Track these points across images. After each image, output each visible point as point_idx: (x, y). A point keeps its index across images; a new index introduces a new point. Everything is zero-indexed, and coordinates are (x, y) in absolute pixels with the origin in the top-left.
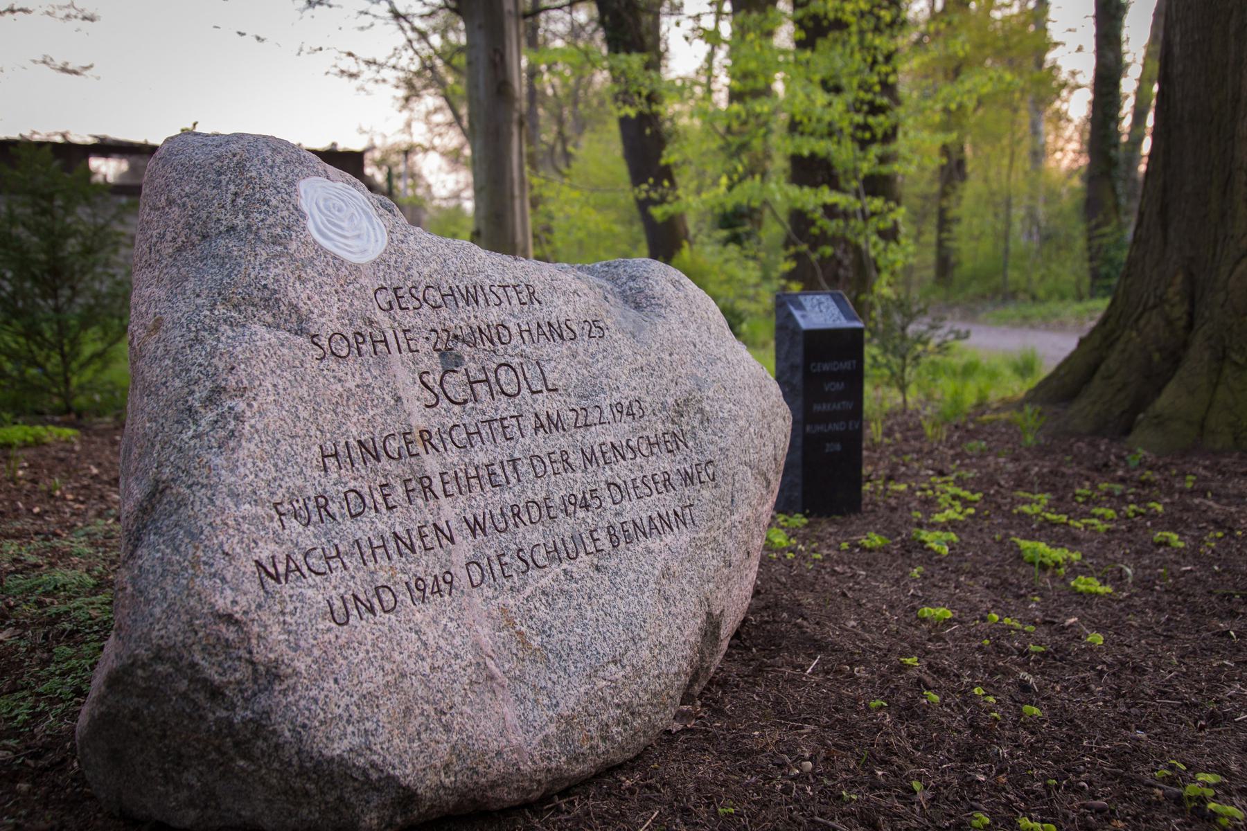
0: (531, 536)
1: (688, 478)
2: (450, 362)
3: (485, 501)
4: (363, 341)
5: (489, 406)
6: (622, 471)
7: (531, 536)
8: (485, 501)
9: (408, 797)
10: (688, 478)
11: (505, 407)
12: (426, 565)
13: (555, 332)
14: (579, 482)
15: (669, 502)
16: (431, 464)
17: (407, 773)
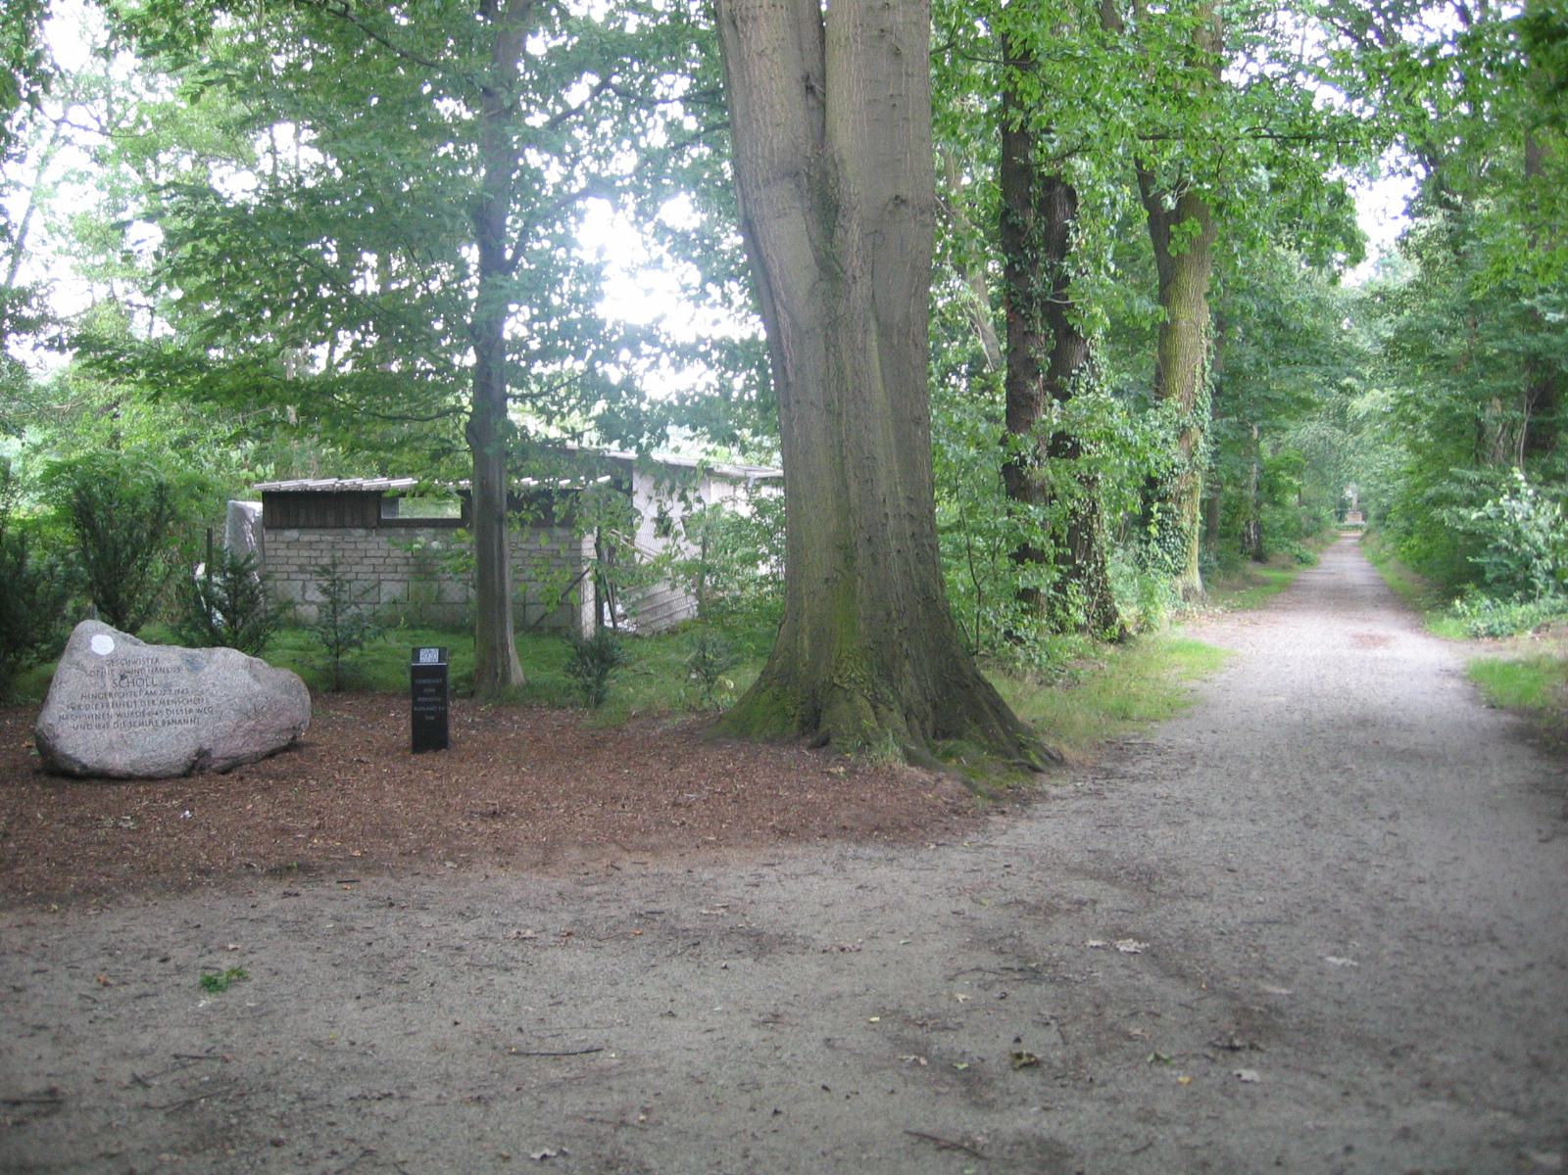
0: (133, 719)
1: (199, 711)
2: (123, 677)
3: (125, 710)
4: (99, 673)
5: (131, 688)
6: (173, 707)
7: (133, 719)
8: (125, 710)
9: (84, 767)
10: (199, 711)
11: (136, 689)
12: (102, 722)
13: (162, 670)
14: (156, 708)
15: (190, 716)
16: (110, 700)
17: (84, 761)
